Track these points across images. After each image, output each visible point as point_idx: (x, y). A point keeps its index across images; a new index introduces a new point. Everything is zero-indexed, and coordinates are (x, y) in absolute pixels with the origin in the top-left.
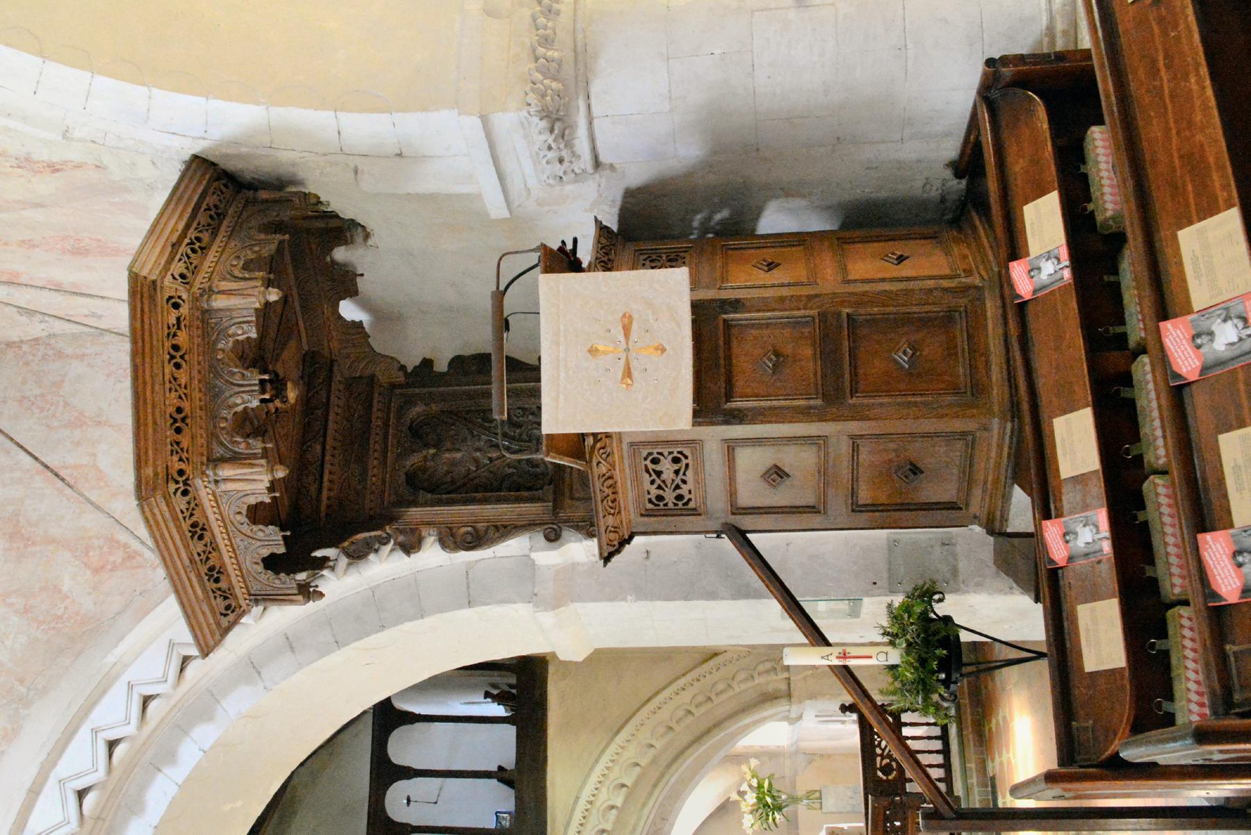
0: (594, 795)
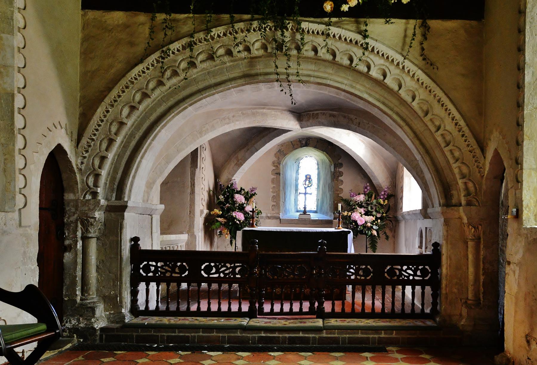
0: (378, 52)
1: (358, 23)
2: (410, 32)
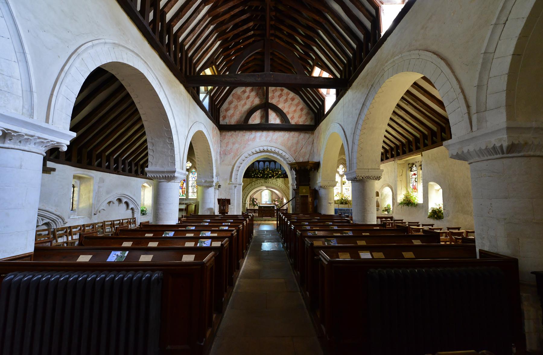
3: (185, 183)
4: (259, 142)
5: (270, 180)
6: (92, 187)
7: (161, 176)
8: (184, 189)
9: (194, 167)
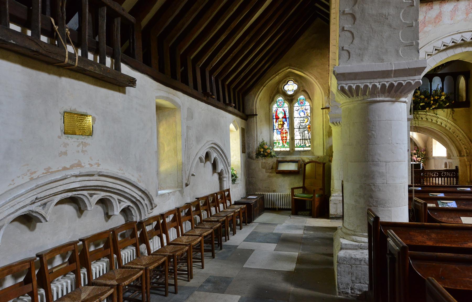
1: (434, 111)
2: (449, 112)
3: (285, 122)
4: (451, 24)
5: (422, 113)
6: (179, 128)
7: (377, 84)
8: (286, 133)
9: (303, 91)
